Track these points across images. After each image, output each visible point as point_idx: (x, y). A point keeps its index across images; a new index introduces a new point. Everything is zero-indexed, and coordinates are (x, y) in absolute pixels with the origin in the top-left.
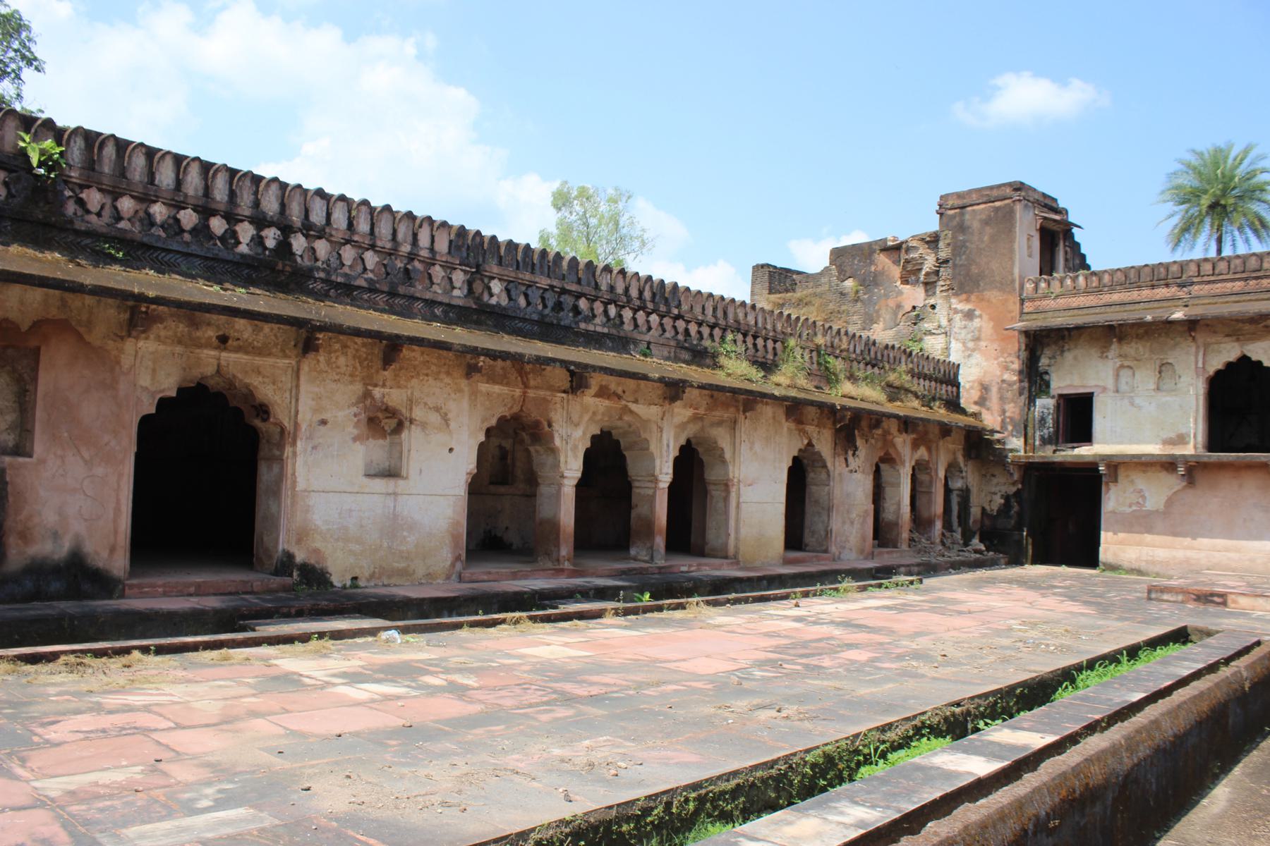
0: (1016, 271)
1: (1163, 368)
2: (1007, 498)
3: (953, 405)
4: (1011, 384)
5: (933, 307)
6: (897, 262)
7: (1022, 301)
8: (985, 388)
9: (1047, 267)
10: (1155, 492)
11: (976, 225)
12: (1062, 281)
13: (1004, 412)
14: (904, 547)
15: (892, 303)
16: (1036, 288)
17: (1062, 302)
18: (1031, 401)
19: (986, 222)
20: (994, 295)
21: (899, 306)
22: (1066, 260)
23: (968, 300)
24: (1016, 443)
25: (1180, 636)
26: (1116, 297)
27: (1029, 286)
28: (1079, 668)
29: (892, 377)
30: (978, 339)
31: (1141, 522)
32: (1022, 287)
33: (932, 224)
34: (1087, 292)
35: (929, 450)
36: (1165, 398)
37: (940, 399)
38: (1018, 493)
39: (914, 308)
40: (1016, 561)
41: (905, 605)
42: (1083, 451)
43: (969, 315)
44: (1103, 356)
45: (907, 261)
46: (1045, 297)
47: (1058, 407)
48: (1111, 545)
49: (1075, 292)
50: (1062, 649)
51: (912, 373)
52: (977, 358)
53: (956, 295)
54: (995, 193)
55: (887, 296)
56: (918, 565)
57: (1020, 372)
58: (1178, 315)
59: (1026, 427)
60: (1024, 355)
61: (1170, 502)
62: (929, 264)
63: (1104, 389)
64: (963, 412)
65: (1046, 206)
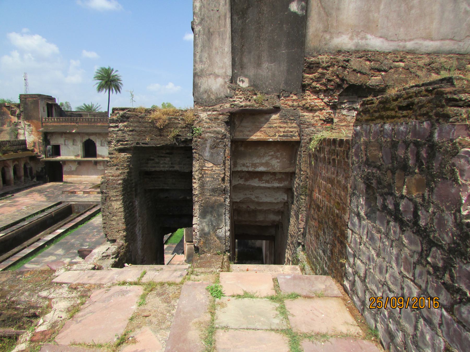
0: (40, 116)
1: (74, 141)
2: (42, 168)
3: (25, 149)
4: (41, 142)
5: (20, 122)
6: (9, 110)
7: (42, 123)
8: (35, 143)
9: (50, 114)
10: (74, 167)
11: (29, 103)
12: (51, 119)
13: (40, 149)
14: (13, 185)
15: (9, 120)
16: (46, 120)
17: (52, 124)
18: (46, 146)
19: (32, 103)
20: (35, 121)
21: (11, 121)
22: (56, 110)
23: (29, 122)
24: (43, 156)
25: (60, 203)
26: (63, 124)
27: (44, 120)
28: (26, 218)
29: (4, 148)
30: (32, 131)
31: (71, 173)
32: (42, 119)
33: (18, 101)
34: (57, 122)
35: (18, 161)
36: (75, 147)
37: (20, 149)
38: (44, 167)
39: (15, 122)
40: (45, 182)
41: (4, 205)
42: (58, 158)
43: (29, 126)
44: (62, 137)
45: (12, 111)
46: (48, 122)
47: (52, 148)
48: (66, 178)
49: (54, 122)
50: (28, 213)
51: (11, 146)
52: (32, 136)
53: (26, 120)
54: (34, 96)
55: (7, 118)
56: (15, 190)
57: (43, 140)
58: (74, 131)
59: (45, 152)
60: (43, 136)
61: (76, 169)
62: (18, 112)
63: (62, 144)
64: (29, 150)
65: (48, 98)
